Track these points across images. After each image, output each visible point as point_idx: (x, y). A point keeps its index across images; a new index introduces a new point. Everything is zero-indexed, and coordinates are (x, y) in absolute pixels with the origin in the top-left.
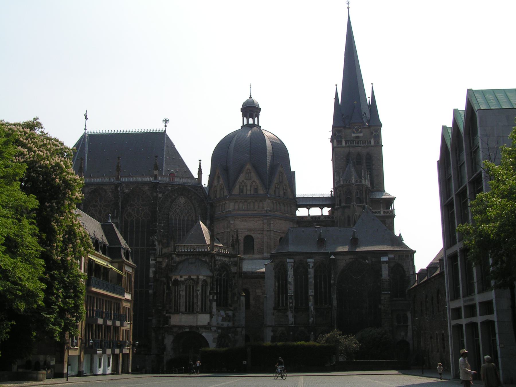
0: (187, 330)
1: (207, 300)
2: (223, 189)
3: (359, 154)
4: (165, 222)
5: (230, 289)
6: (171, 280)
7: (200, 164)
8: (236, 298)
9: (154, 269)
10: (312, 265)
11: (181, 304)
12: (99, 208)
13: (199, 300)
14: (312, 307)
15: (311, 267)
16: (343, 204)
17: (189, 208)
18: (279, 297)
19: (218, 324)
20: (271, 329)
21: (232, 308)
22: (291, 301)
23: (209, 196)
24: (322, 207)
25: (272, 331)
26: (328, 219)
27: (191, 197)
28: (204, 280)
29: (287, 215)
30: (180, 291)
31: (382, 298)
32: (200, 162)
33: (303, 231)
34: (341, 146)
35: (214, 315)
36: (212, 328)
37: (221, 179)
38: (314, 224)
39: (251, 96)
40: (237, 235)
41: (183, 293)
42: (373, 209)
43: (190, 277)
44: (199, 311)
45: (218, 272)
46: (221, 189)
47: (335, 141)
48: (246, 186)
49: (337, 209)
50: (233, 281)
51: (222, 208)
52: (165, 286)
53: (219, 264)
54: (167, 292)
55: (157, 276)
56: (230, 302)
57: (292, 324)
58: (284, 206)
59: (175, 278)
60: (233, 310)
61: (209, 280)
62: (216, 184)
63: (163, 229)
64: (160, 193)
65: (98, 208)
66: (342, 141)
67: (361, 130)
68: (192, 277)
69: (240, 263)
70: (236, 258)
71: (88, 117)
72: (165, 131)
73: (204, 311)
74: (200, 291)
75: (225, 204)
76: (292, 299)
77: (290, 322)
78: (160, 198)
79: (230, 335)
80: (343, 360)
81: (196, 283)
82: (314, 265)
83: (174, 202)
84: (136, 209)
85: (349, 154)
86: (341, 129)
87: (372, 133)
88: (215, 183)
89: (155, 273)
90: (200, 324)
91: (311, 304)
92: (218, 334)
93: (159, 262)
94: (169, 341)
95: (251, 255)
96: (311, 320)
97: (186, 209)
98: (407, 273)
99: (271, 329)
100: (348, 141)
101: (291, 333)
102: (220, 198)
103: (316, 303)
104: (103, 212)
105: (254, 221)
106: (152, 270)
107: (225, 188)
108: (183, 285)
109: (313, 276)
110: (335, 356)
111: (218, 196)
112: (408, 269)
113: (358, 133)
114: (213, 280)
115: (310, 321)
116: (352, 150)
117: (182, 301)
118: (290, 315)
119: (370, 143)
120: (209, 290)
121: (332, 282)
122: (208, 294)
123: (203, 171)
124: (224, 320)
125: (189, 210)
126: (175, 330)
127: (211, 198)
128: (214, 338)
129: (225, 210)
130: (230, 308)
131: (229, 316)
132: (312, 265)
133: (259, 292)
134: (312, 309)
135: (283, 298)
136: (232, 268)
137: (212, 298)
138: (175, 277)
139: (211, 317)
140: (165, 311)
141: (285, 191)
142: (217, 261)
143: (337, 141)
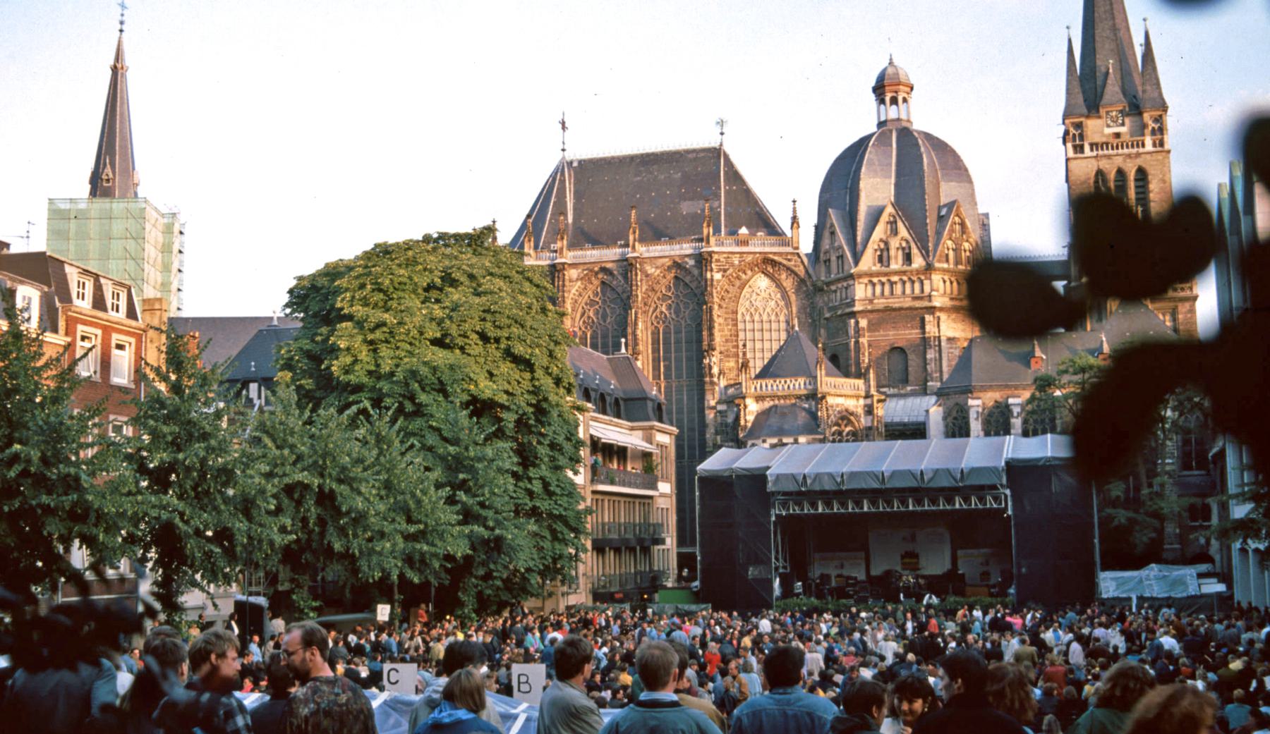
7: (794, 210)
10: (1016, 410)
15: (1015, 414)
39: (891, 59)
43: (781, 440)
47: (1069, 145)
71: (566, 125)
72: (721, 145)
75: (846, 288)
78: (718, 281)
82: (1023, 409)
87: (1144, 126)
93: (720, 412)
100: (1097, 144)
116: (1104, 165)
119: (1143, 145)
143: (1075, 147)
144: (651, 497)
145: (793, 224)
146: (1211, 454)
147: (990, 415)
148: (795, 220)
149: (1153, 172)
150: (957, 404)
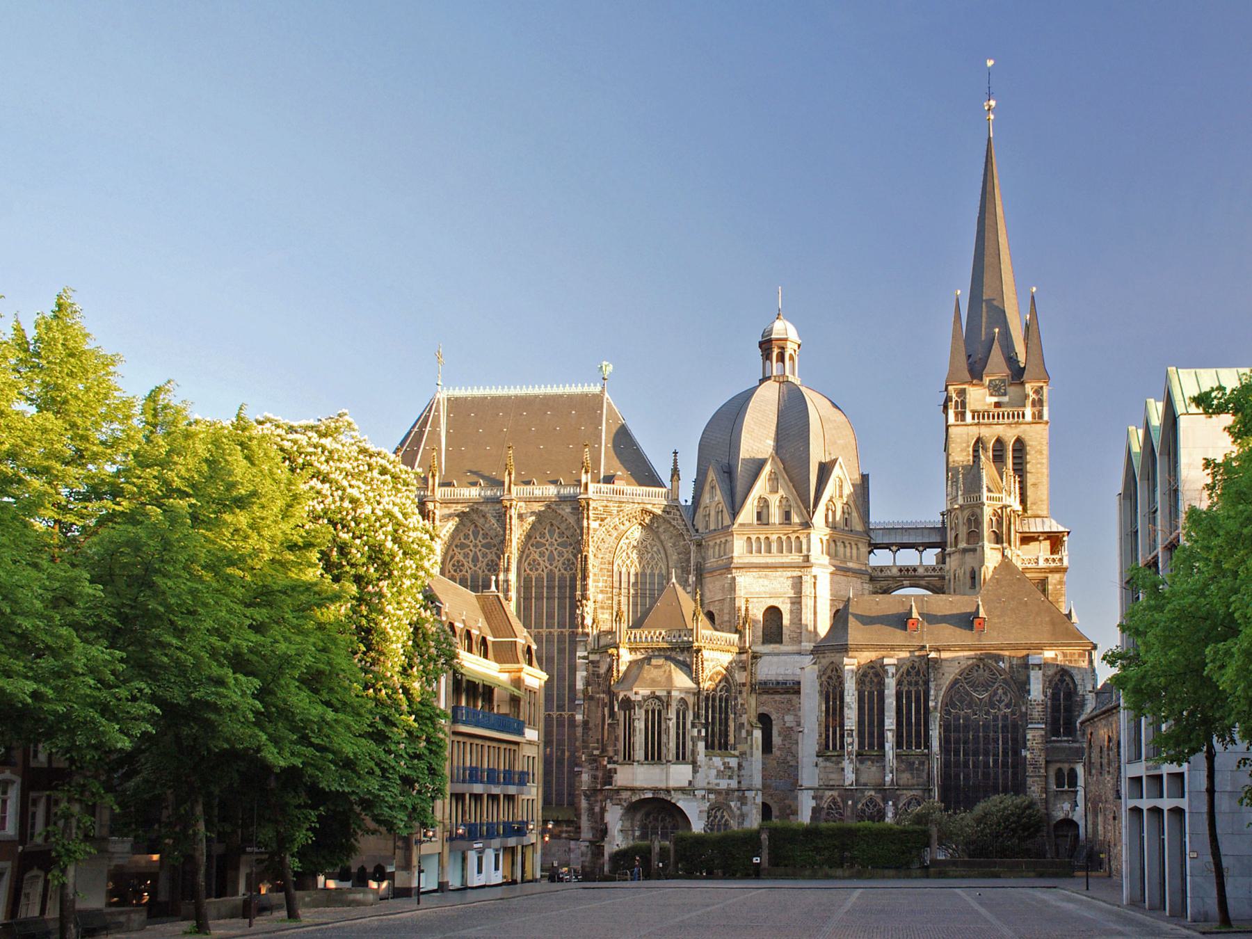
0: (650, 795)
1: (688, 738)
2: (722, 511)
3: (999, 442)
4: (605, 578)
5: (732, 716)
6: (617, 700)
7: (675, 461)
8: (744, 733)
9: (585, 673)
10: (892, 670)
11: (637, 746)
12: (473, 549)
13: (671, 737)
14: (891, 752)
15: (890, 675)
16: (962, 545)
17: (655, 549)
18: (827, 730)
19: (708, 783)
20: (811, 793)
21: (737, 753)
22: (850, 740)
23: (694, 526)
24: (920, 547)
25: (813, 798)
26: (933, 574)
27: (658, 527)
28: (682, 698)
29: (850, 565)
30: (634, 720)
31: (1029, 737)
32: (675, 456)
33: (877, 603)
34: (962, 423)
35: (700, 767)
36: (696, 792)
37: (718, 492)
38: (905, 582)
40: (747, 609)
41: (640, 725)
42: (1023, 555)
44: (671, 759)
45: (710, 682)
46: (718, 512)
48: (768, 506)
49: (950, 554)
50: (740, 701)
51: (719, 551)
52: (606, 710)
53: (711, 667)
54: (610, 721)
55: (590, 688)
56: (731, 740)
57: (852, 785)
58: (845, 547)
59: (625, 696)
60: (737, 757)
61: (691, 700)
62: (708, 501)
63: (602, 592)
64: (595, 520)
65: (471, 550)
66: (965, 412)
67: (1005, 390)
68: (657, 694)
69: (752, 664)
70: (745, 655)
73: (681, 757)
74: (674, 720)
76: (852, 736)
77: (847, 782)
78: (595, 530)
79: (732, 804)
80: (944, 858)
81: (665, 704)
82: (897, 671)
83: (624, 537)
84: (547, 553)
85: (978, 440)
86: (964, 387)
87: (1027, 396)
88: (706, 499)
89: (587, 684)
90: (672, 784)
91: (888, 746)
92: (708, 804)
93: (592, 662)
94: (614, 817)
95: (777, 646)
96: (888, 778)
97: (648, 553)
98: (1079, 687)
99: (811, 793)
100: (979, 412)
101: (850, 802)
102: (715, 530)
103: (899, 744)
104: (480, 558)
105: (781, 576)
106: (581, 675)
107: (725, 509)
108: (640, 708)
109: (894, 692)
110: (928, 849)
111: (712, 527)
112: (1083, 680)
113: (999, 395)
114: (698, 698)
115: (887, 779)
117: (639, 739)
118: (848, 767)
119: (1023, 417)
120: (691, 718)
121: (931, 704)
122: (689, 725)
123: (680, 473)
124: (720, 774)
125: (655, 555)
126: (625, 795)
127: (697, 531)
128: (700, 812)
129: (725, 555)
130: (733, 752)
131: (730, 768)
132: (892, 670)
133: (789, 719)
134: (891, 758)
135: (835, 733)
136: (736, 675)
137: (696, 734)
138: (625, 693)
139: (695, 771)
140: (606, 759)
141: (846, 516)
142: (707, 660)
143: (956, 414)
144: (517, 743)
145: (672, 476)
146: (1079, 721)
147: (865, 675)
148: (675, 472)
149: (1030, 443)
150: (832, 662)
